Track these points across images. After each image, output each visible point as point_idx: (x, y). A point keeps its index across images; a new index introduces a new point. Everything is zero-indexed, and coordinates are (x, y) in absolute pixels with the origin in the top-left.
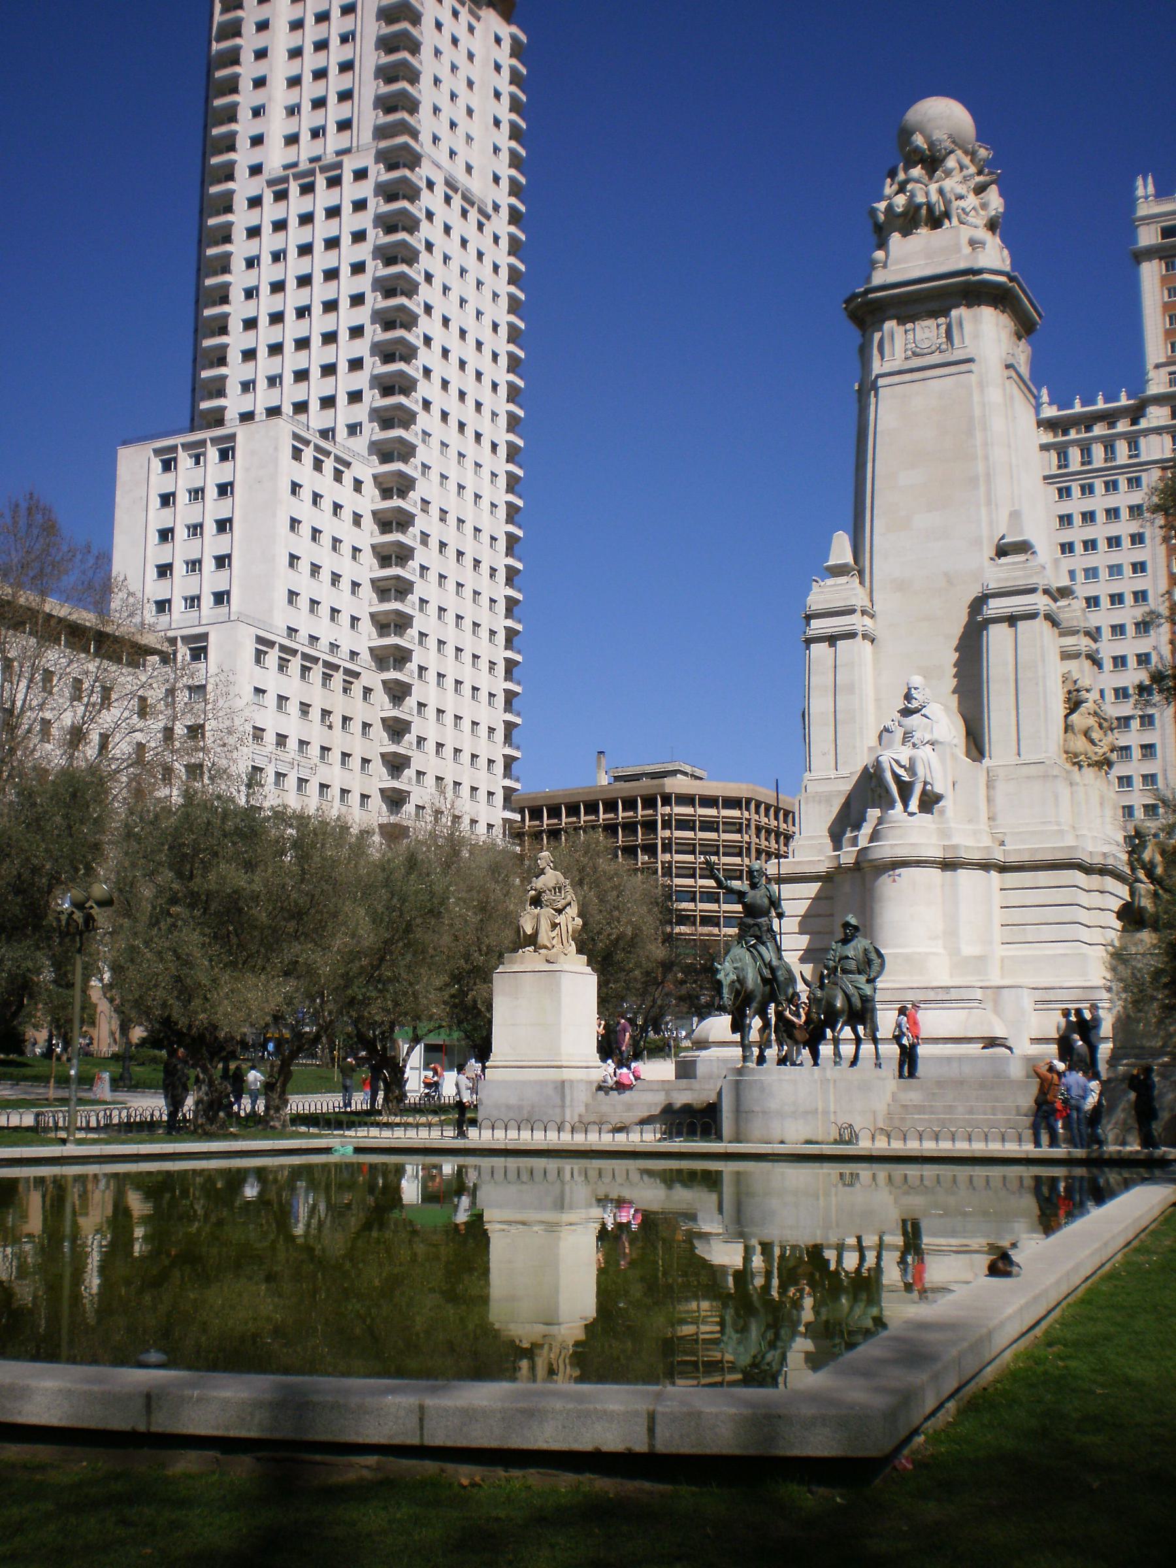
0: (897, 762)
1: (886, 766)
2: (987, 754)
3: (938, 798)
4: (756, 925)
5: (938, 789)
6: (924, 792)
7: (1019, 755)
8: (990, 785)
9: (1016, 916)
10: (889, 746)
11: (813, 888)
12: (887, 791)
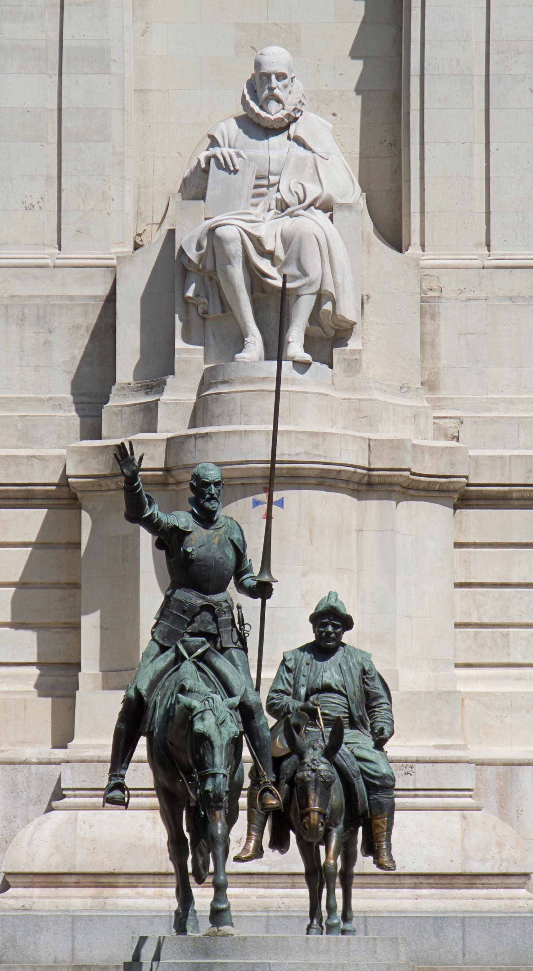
0: (257, 242)
1: (235, 249)
2: (415, 238)
3: (341, 333)
4: (209, 608)
5: (348, 310)
6: (315, 317)
7: (488, 245)
8: (428, 308)
9: (489, 606)
10: (226, 204)
11: (29, 523)
12: (226, 307)
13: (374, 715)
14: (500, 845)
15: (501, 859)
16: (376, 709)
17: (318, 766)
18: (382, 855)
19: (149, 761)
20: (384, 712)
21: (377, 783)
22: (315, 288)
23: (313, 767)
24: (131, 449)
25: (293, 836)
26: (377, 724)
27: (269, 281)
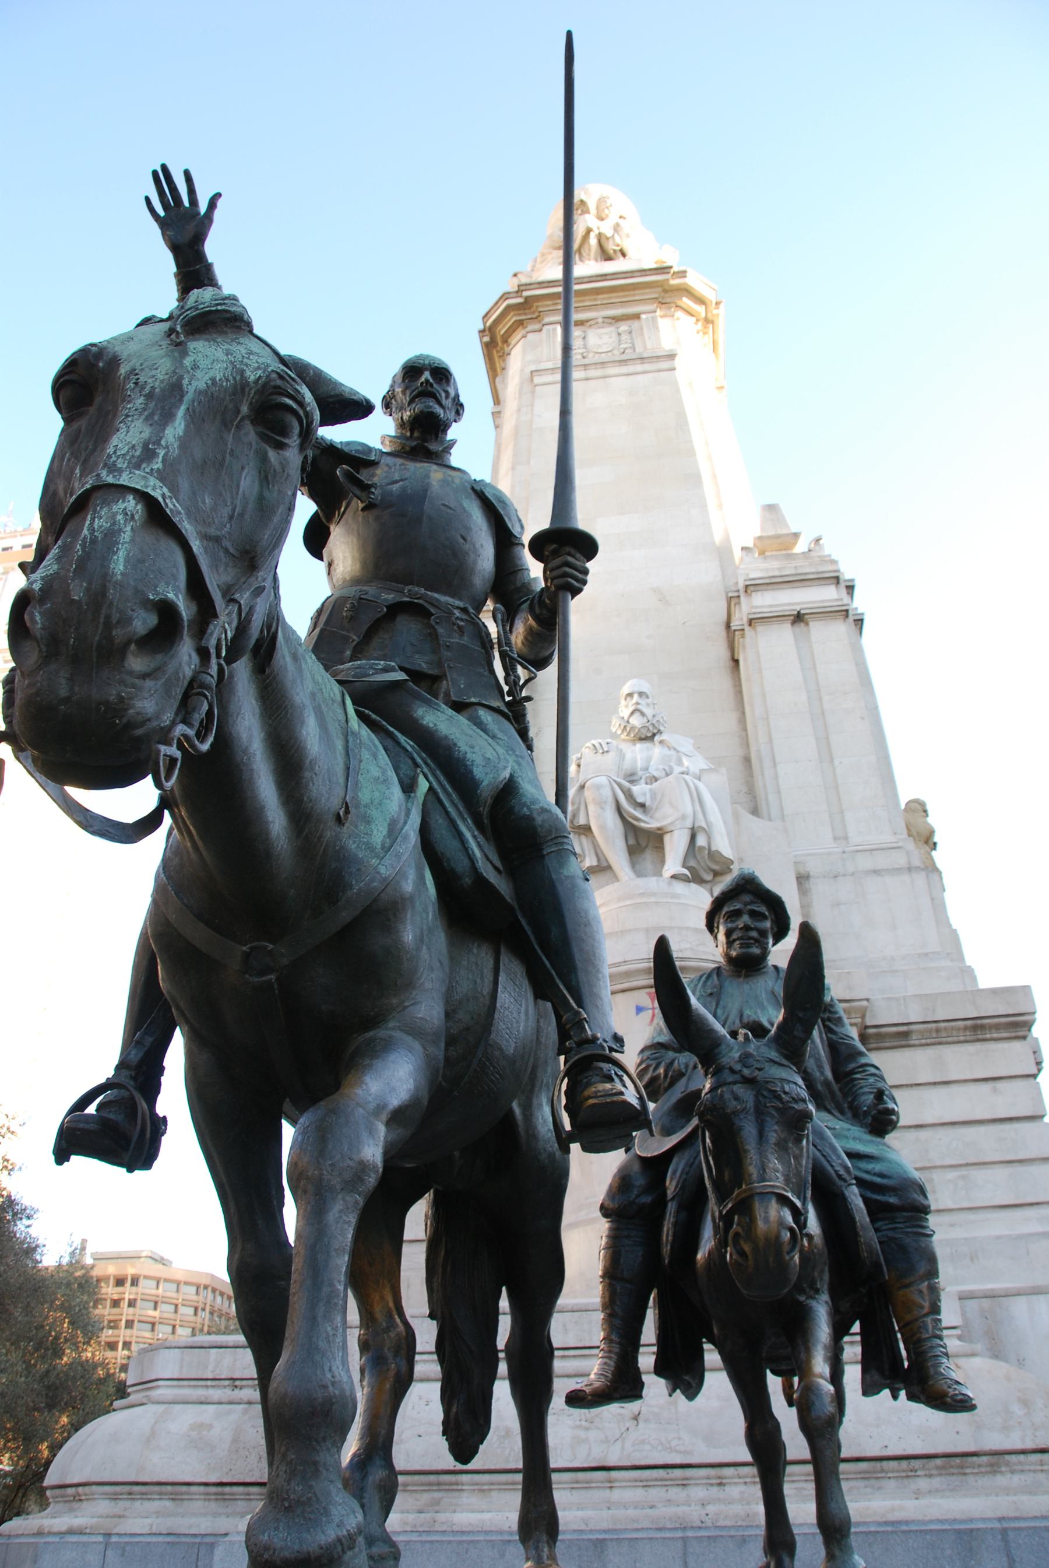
13: (854, 1085)
14: (1025, 1403)
15: (1033, 1425)
16: (858, 1076)
17: (760, 1070)
18: (932, 1372)
19: (552, 1350)
20: (872, 1080)
21: (892, 1200)
22: (689, 824)
23: (746, 1072)
24: (192, 191)
25: (712, 1356)
26: (863, 1098)
27: (643, 825)
